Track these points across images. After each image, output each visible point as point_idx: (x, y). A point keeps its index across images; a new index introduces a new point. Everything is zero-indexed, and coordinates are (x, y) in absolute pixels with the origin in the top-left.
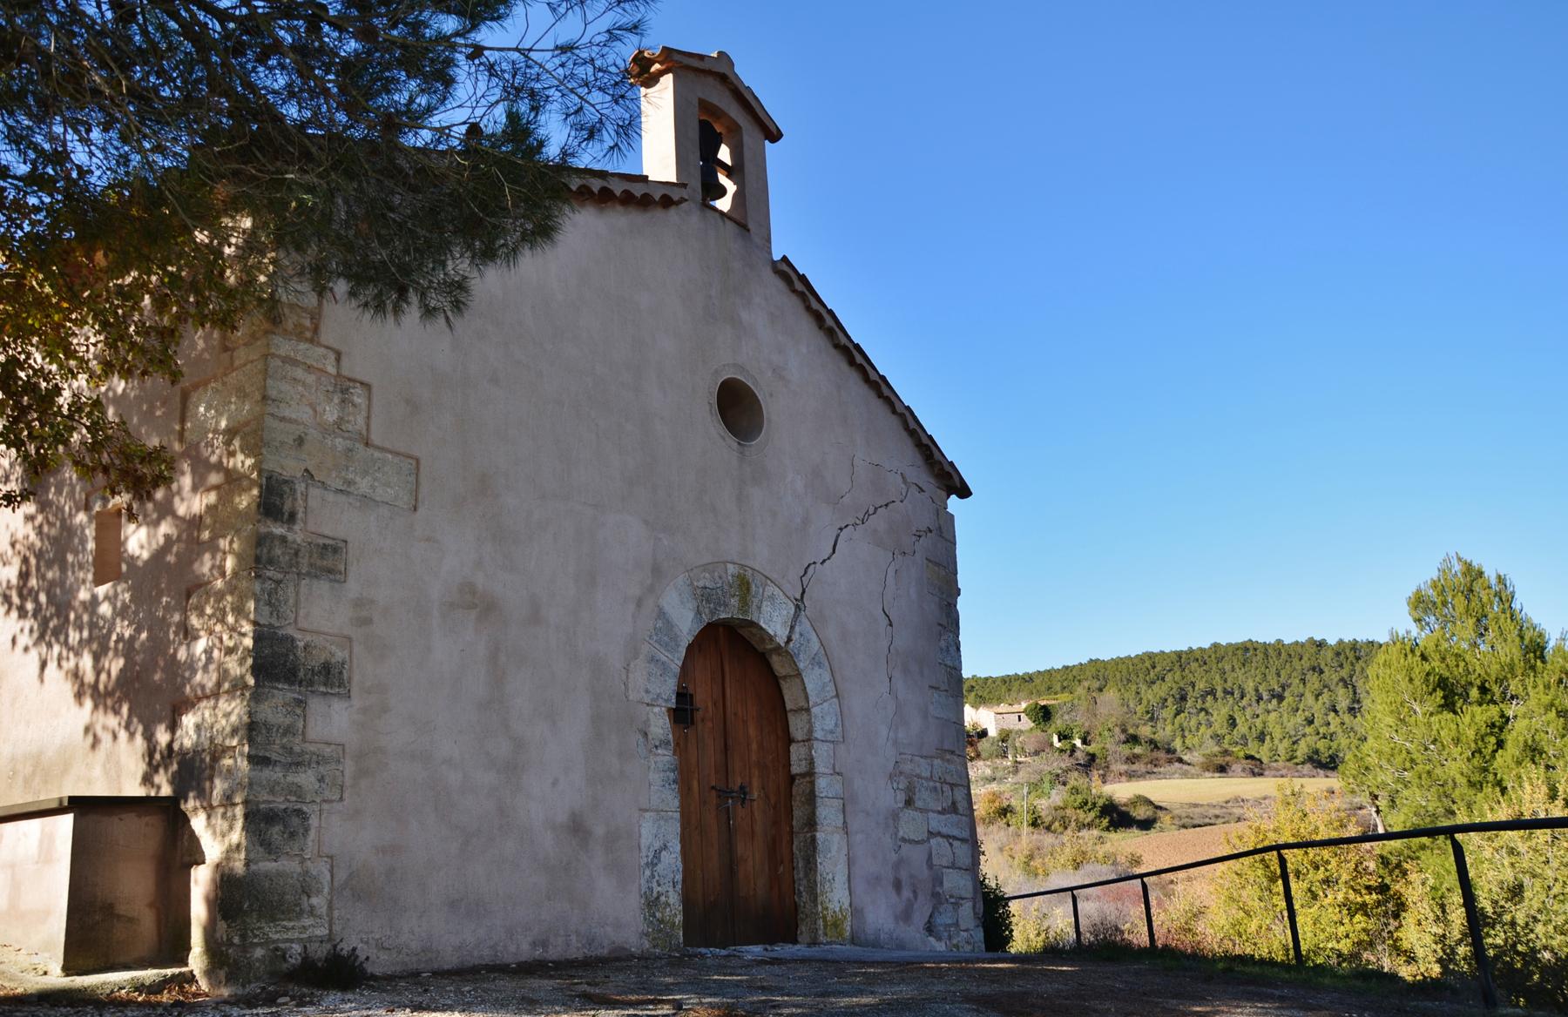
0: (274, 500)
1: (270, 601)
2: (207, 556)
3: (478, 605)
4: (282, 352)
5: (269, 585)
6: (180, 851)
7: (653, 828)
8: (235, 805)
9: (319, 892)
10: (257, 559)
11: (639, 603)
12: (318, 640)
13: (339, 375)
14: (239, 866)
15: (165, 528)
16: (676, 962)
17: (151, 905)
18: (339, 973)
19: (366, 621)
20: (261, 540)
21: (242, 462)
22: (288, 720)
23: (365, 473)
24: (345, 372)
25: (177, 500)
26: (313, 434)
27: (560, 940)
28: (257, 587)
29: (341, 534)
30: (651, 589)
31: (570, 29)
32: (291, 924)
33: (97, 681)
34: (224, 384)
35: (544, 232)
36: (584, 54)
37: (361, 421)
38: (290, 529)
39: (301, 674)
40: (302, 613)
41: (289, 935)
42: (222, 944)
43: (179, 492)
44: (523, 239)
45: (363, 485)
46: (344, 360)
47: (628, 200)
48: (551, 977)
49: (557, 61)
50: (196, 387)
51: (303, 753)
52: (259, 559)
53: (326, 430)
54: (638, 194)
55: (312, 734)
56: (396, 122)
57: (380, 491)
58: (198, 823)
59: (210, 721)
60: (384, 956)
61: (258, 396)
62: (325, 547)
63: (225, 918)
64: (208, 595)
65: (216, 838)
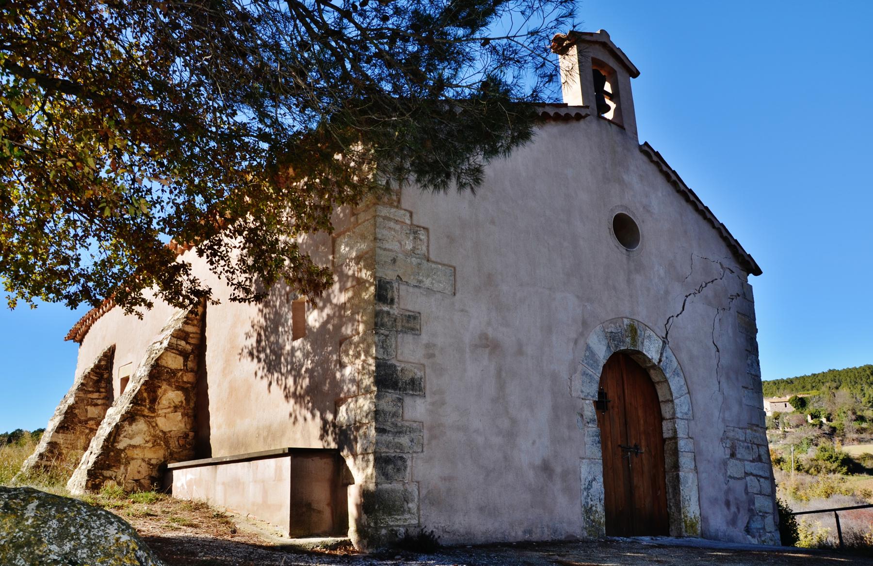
0: (383, 294)
1: (383, 346)
2: (350, 326)
3: (488, 345)
4: (383, 214)
5: (382, 338)
6: (341, 478)
7: (589, 469)
8: (368, 454)
9: (413, 500)
10: (376, 324)
11: (576, 342)
12: (408, 366)
13: (412, 224)
14: (372, 487)
15: (328, 311)
16: (606, 544)
17: (328, 505)
18: (423, 544)
19: (431, 356)
20: (377, 314)
21: (365, 274)
22: (394, 409)
23: (428, 276)
24: (415, 223)
25: (332, 296)
26: (401, 256)
27: (539, 530)
28: (376, 339)
29: (417, 310)
30: (582, 334)
31: (535, 22)
32: (399, 517)
33: (296, 389)
34: (354, 233)
35: (524, 136)
36: (544, 35)
37: (424, 248)
38: (391, 308)
39: (400, 384)
40: (399, 352)
41: (399, 523)
42: (365, 526)
43: (333, 292)
44: (512, 142)
45: (427, 282)
46: (414, 216)
47: (557, 118)
48: (537, 551)
49: (529, 40)
50: (339, 235)
51: (402, 426)
52: (377, 324)
53: (407, 254)
54: (563, 114)
55: (406, 417)
56: (441, 84)
57: (436, 285)
58: (350, 462)
59: (358, 408)
60: (446, 536)
61: (371, 238)
62: (409, 316)
63: (366, 513)
64: (351, 344)
65: (361, 473)
